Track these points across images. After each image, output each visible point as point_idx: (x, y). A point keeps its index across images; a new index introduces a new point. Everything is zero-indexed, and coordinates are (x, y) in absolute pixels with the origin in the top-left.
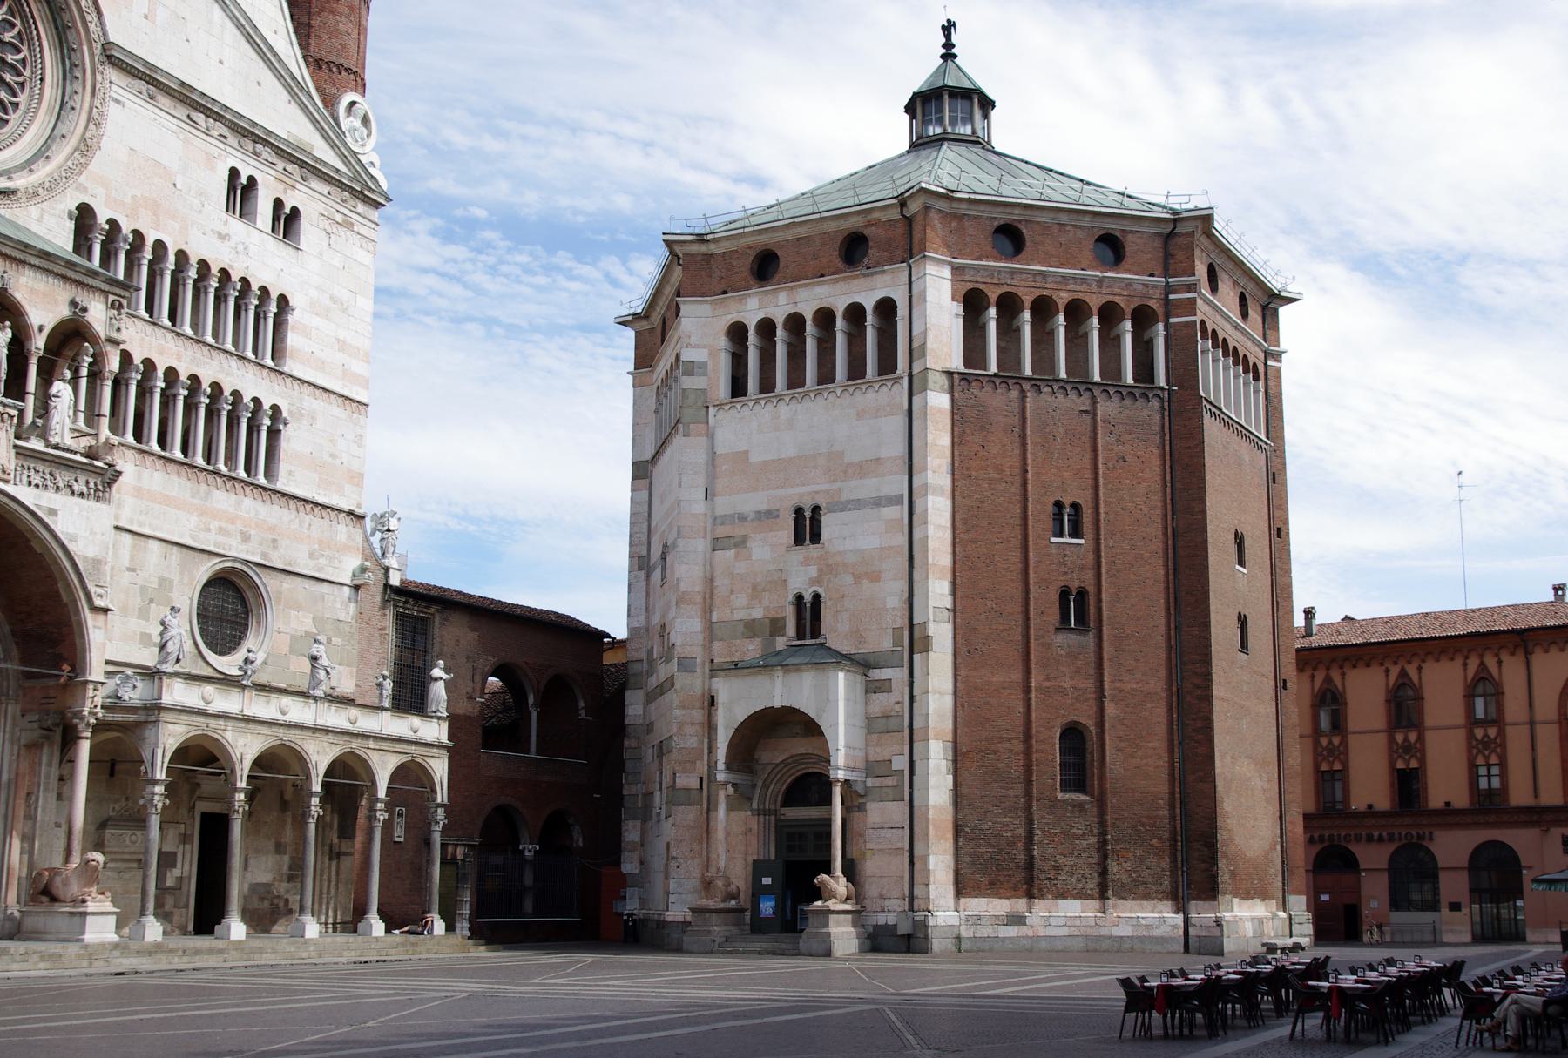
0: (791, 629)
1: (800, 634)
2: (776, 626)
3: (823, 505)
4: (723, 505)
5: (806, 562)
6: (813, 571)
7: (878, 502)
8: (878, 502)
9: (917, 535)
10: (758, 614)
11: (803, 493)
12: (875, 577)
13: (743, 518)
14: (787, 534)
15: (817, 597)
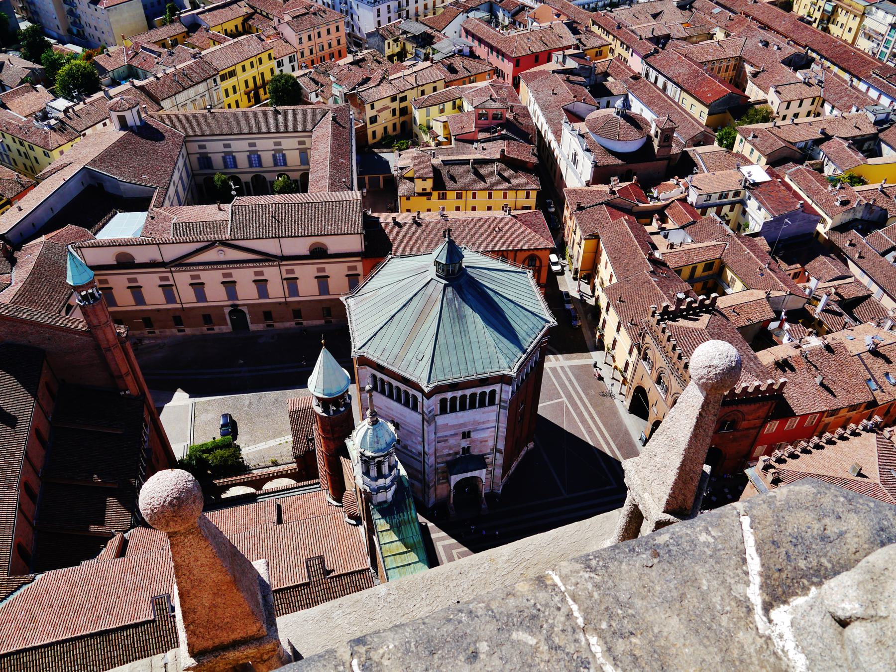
0: (461, 453)
2: (457, 453)
4: (439, 434)
6: (468, 443)
7: (488, 428)
8: (488, 428)
9: (499, 433)
10: (451, 452)
11: (466, 429)
13: (446, 436)
14: (461, 437)
15: (469, 447)
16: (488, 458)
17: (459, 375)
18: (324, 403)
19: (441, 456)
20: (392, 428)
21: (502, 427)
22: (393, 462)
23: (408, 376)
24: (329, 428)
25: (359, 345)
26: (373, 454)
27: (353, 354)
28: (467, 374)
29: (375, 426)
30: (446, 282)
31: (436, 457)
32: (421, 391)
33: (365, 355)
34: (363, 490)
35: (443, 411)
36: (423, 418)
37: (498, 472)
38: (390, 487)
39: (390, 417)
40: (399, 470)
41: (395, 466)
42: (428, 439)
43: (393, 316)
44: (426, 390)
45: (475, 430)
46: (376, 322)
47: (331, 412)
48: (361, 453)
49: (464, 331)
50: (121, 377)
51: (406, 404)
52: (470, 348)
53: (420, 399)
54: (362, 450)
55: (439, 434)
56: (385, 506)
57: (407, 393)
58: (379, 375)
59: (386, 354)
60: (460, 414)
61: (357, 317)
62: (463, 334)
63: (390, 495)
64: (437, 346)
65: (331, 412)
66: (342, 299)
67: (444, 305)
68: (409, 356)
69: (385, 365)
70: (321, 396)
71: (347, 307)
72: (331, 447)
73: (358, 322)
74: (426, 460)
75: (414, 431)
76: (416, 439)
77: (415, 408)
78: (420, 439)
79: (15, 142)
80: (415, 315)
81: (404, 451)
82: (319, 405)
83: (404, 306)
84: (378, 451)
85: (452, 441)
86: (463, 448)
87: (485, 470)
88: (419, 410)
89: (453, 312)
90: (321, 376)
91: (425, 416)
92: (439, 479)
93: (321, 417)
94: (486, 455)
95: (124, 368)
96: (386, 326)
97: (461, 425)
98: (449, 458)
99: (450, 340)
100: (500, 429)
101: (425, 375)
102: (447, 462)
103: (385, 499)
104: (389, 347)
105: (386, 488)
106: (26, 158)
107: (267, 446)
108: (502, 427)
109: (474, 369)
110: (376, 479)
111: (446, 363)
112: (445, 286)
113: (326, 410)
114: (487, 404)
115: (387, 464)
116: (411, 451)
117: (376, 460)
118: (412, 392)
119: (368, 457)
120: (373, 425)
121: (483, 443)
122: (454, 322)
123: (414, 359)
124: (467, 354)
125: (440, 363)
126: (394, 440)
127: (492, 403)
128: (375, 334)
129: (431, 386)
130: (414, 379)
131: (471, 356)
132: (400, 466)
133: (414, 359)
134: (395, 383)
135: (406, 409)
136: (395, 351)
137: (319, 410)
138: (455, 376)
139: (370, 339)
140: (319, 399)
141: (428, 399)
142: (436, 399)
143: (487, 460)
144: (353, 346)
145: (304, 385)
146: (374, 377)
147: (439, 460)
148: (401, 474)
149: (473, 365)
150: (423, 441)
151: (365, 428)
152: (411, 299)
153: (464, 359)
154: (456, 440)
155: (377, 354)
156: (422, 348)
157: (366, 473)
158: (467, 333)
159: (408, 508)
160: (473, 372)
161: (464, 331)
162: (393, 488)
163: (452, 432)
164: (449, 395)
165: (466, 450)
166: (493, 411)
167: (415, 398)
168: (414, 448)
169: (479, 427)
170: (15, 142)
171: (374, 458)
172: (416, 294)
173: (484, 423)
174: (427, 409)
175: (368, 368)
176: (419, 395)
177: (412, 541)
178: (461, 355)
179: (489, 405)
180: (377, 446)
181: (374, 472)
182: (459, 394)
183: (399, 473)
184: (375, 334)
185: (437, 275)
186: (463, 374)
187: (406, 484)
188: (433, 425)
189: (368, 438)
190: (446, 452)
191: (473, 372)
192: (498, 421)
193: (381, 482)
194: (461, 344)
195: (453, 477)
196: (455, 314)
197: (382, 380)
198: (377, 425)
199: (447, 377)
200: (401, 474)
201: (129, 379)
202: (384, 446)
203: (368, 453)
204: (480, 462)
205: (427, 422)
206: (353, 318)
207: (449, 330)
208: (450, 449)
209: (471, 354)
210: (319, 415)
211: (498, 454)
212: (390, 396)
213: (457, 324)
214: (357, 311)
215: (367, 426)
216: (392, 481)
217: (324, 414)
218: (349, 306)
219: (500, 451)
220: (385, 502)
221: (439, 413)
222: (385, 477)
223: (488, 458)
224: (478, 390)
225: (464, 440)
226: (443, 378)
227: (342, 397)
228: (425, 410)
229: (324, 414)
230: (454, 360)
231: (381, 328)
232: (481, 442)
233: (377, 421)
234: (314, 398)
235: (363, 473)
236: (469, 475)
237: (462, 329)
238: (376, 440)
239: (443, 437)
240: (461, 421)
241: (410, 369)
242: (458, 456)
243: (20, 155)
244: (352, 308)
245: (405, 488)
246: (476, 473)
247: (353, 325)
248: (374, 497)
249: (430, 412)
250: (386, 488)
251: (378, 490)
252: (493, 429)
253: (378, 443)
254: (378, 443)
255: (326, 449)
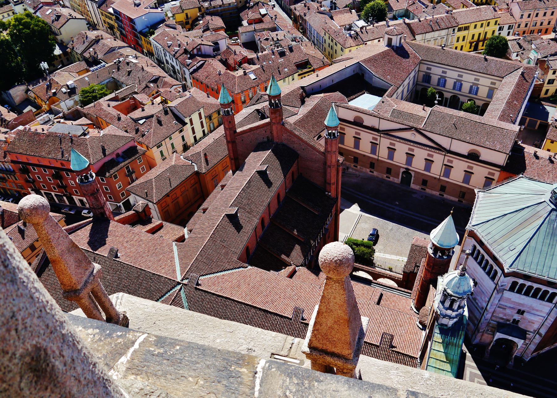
0: (511, 322)
1: (512, 323)
2: (508, 320)
3: (526, 311)
4: (501, 303)
5: (519, 316)
6: (520, 318)
7: (539, 316)
8: (539, 316)
9: (546, 323)
10: (505, 318)
11: (522, 309)
12: (534, 323)
13: (506, 306)
15: (518, 321)
16: (530, 335)
17: (534, 272)
18: (436, 249)
19: (497, 317)
20: (472, 283)
21: (550, 320)
22: (462, 304)
23: (498, 257)
24: (432, 264)
25: (473, 223)
26: (452, 293)
27: (467, 227)
28: (540, 274)
29: (461, 277)
30: (554, 207)
31: (492, 315)
32: (503, 270)
33: (475, 231)
34: (435, 311)
35: (512, 289)
36: (496, 288)
37: (532, 347)
38: (454, 318)
39: (473, 276)
40: (464, 311)
41: (463, 308)
42: (493, 302)
43: (505, 215)
44: (506, 271)
45: (528, 312)
46: (492, 214)
47: (438, 256)
48: (445, 289)
49: (553, 245)
50: (330, 184)
51: (488, 274)
52: (551, 257)
53: (499, 274)
54: (446, 288)
55: (501, 303)
56: (445, 328)
57: (492, 267)
58: (478, 247)
59: (490, 236)
60: (524, 297)
61: (481, 205)
62: (550, 246)
63: (451, 323)
64: (527, 246)
65: (438, 256)
66: (476, 191)
67: (545, 222)
68: (505, 244)
69: (486, 243)
70: (435, 243)
71: (476, 197)
72: (428, 277)
73: (480, 209)
74: (485, 314)
75: (485, 293)
76: (485, 298)
77: (493, 278)
78: (487, 299)
79: (329, 39)
80: (521, 220)
81: (473, 301)
82: (431, 248)
83: (516, 211)
84: (457, 293)
85: (508, 311)
86: (514, 320)
87: (523, 341)
88: (496, 281)
89: (550, 229)
90: (441, 232)
91: (497, 287)
92: (488, 330)
93: (430, 256)
94: (529, 331)
95: (333, 180)
96: (498, 219)
97: (520, 304)
98: (501, 321)
99: (539, 247)
100: (548, 320)
101: (510, 261)
102: (499, 323)
103: (446, 324)
104: (494, 233)
105: (450, 318)
106: (332, 49)
107: (390, 258)
108: (550, 320)
109: (547, 273)
110: (447, 309)
111: (529, 260)
112: (553, 210)
113: (435, 253)
114: (546, 300)
115: (458, 303)
116: (477, 304)
117: (453, 298)
118: (495, 267)
119: (448, 294)
120: (460, 276)
121: (531, 324)
122: (547, 236)
123: (507, 248)
124: (547, 261)
125: (524, 258)
126: (469, 291)
127: (550, 300)
128: (488, 221)
129: (511, 270)
130: (501, 260)
131: (550, 263)
132: (466, 309)
133: (507, 248)
134: (487, 257)
135: (487, 276)
136: (497, 237)
137: (431, 251)
138: (531, 271)
139: (483, 223)
140: (433, 244)
141: (505, 277)
142: (511, 279)
143: (527, 336)
144: (469, 222)
145: (428, 232)
146: (475, 247)
147: (493, 318)
148: (464, 314)
149: (548, 270)
150: (489, 302)
151: (454, 275)
152: (524, 209)
153: (543, 263)
154: (512, 312)
155: (483, 234)
156: (516, 243)
157: (443, 302)
158: (554, 247)
159: (459, 337)
160: (546, 275)
161: (553, 245)
162: (455, 320)
163: (512, 306)
164: (521, 281)
165: (516, 322)
166: (548, 306)
167: (496, 273)
168: (480, 303)
169: (533, 312)
170: (329, 39)
171: (451, 296)
172: (528, 207)
173: (537, 310)
174: (501, 283)
175: (473, 239)
176: (500, 272)
177: (452, 358)
178: (542, 259)
179: (547, 301)
180: (456, 290)
181: (447, 304)
182: (528, 284)
183: (463, 313)
184: (488, 221)
185: (550, 200)
186: (538, 273)
187: (465, 322)
188: (500, 295)
189: (453, 282)
190: (501, 315)
191: (546, 275)
192: (549, 314)
193: (449, 312)
194: (546, 252)
195: (498, 334)
196: (551, 231)
197: (479, 251)
198: (463, 277)
199: (525, 269)
200: (464, 314)
201: (333, 187)
202: (461, 292)
203: (449, 291)
204: (522, 334)
205: (497, 291)
206: (478, 205)
207: (541, 239)
208: (505, 315)
209: (550, 262)
210: (429, 254)
211: (537, 336)
212: (480, 264)
213: (549, 238)
214: (482, 202)
215: (456, 275)
216: (457, 316)
217: (432, 255)
218: (478, 197)
219: (540, 335)
220: (446, 325)
221: (508, 289)
222: (453, 311)
223: (530, 335)
224: (544, 288)
225: (518, 315)
226: (522, 269)
227: (449, 250)
228: (499, 283)
229: (432, 255)
230: (536, 260)
231: (494, 219)
232: (529, 322)
233: (464, 275)
234: (431, 243)
235: (440, 301)
236: (510, 338)
237: (551, 243)
238: (458, 285)
239: (503, 305)
240: (521, 302)
241: (501, 253)
242: (508, 323)
243: (329, 46)
244: (480, 199)
245: (462, 324)
246: (515, 340)
247: (476, 209)
248: (440, 319)
249: (502, 286)
250: (450, 318)
251: (445, 316)
252: (542, 318)
253: (458, 288)
254: (458, 288)
255: (424, 276)
